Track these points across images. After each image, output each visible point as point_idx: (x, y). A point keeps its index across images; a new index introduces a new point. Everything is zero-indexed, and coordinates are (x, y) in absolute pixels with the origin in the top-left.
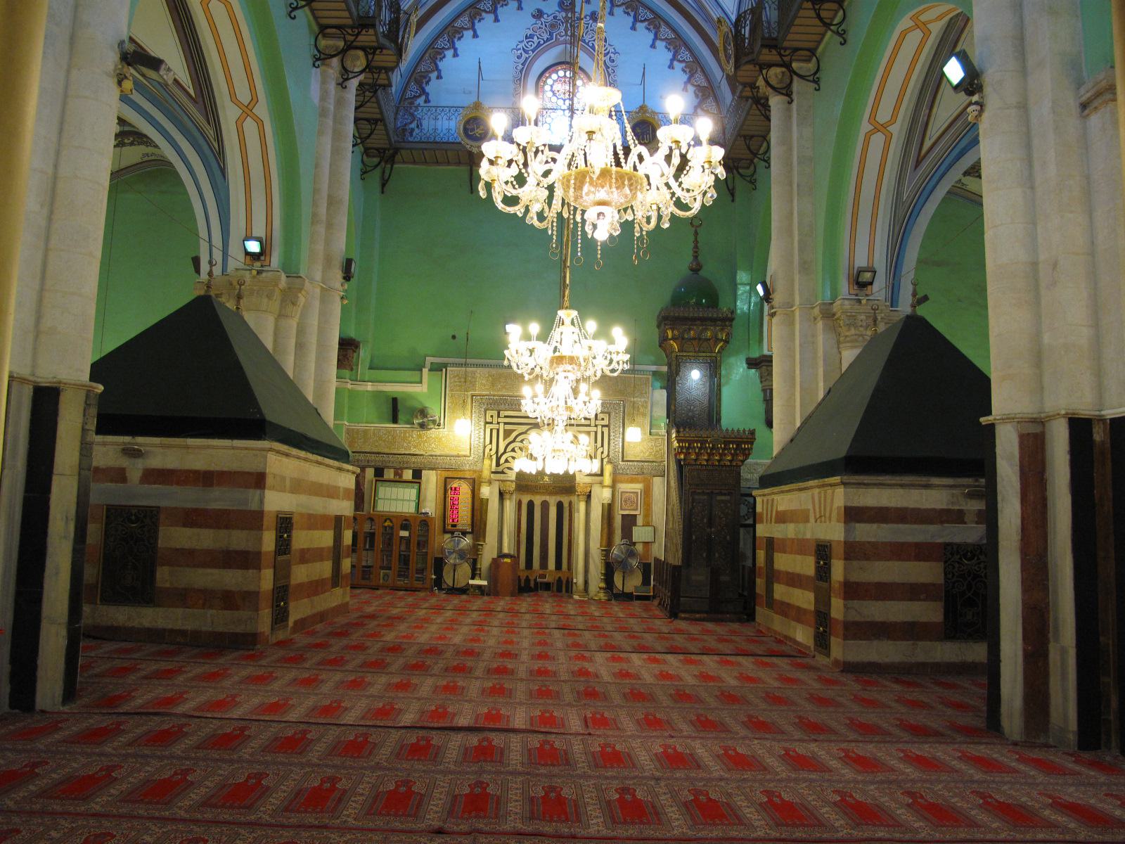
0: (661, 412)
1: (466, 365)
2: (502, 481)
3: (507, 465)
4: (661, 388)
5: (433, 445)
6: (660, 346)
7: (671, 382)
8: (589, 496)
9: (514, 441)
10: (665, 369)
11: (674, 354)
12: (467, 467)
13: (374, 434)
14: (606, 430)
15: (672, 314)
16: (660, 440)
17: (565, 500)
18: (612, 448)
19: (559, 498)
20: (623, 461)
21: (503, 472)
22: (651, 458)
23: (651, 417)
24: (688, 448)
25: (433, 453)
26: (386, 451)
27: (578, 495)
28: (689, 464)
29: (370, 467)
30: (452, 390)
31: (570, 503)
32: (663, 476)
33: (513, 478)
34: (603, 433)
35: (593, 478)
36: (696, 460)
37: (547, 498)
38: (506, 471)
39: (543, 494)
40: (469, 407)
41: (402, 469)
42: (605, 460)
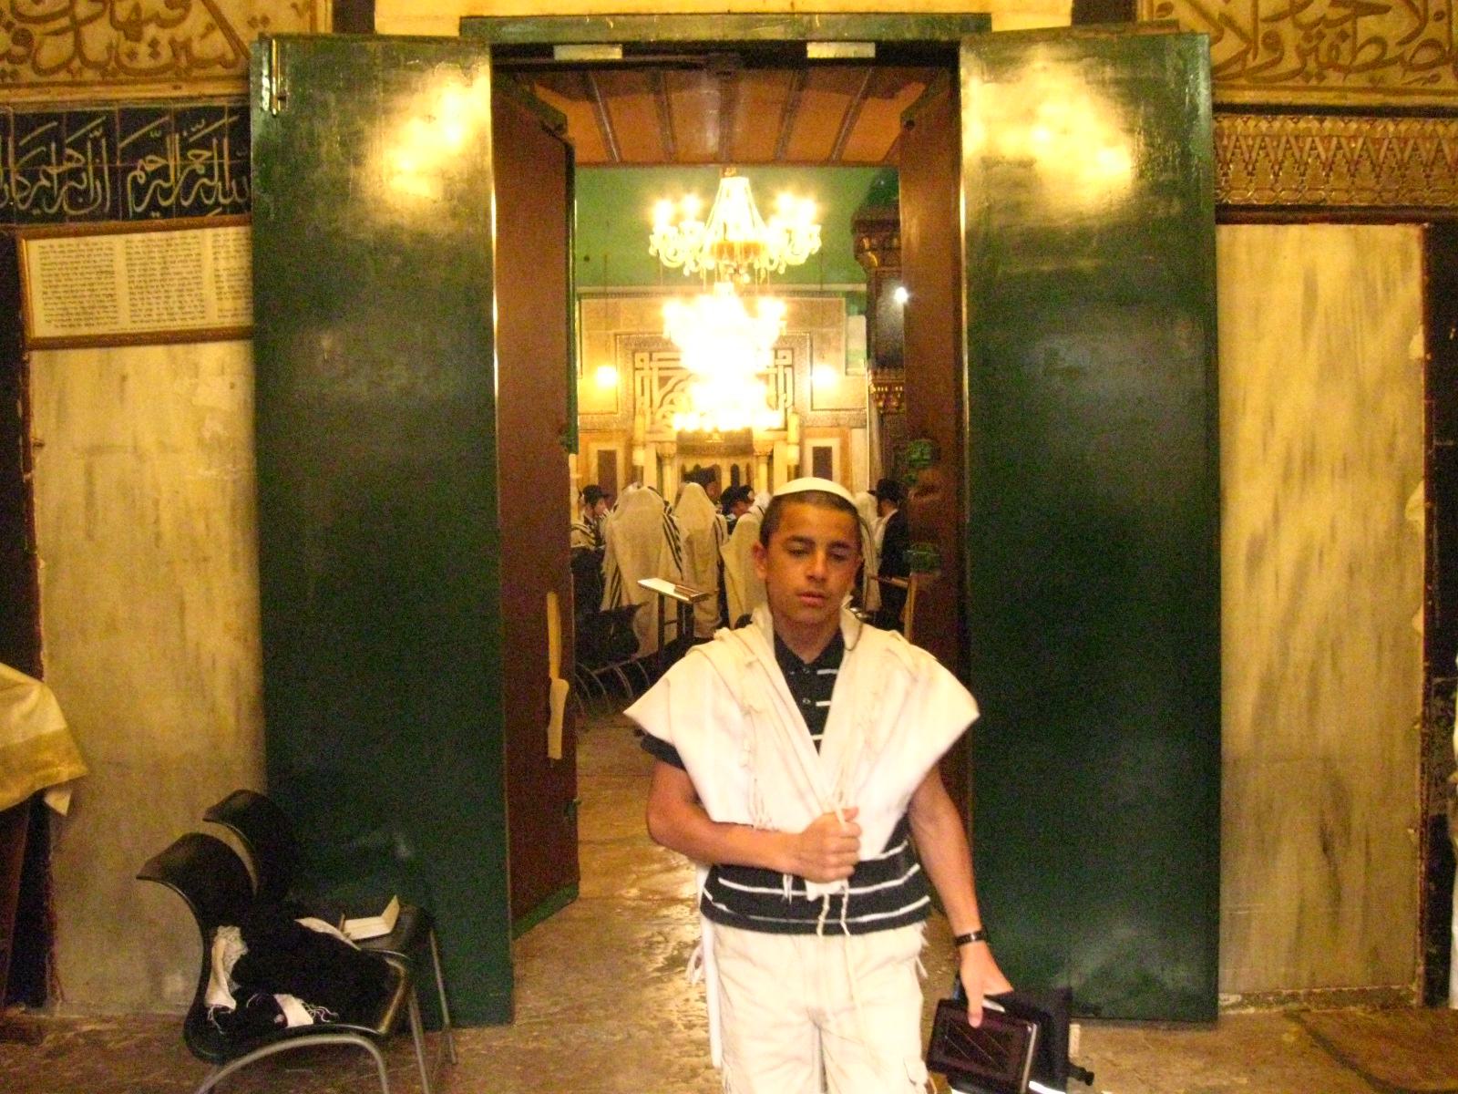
0: (859, 345)
1: (605, 295)
2: (660, 442)
4: (860, 313)
6: (856, 258)
7: (871, 306)
8: (771, 457)
9: (671, 391)
10: (863, 288)
11: (873, 270)
12: (615, 426)
15: (868, 217)
17: (742, 463)
19: (733, 461)
20: (812, 410)
23: (847, 352)
24: (887, 394)
27: (757, 457)
28: (889, 413)
30: (587, 330)
31: (748, 467)
32: (864, 427)
33: (674, 437)
34: (785, 375)
36: (898, 408)
37: (718, 461)
39: (713, 456)
40: (613, 349)
42: (790, 411)
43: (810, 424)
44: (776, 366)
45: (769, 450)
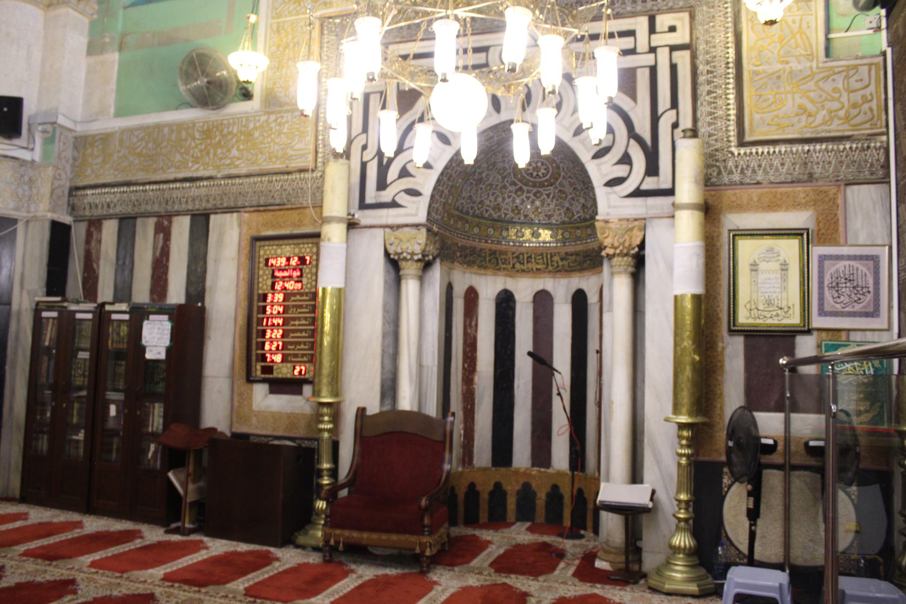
2: (391, 227)
3: (406, 183)
5: (234, 152)
8: (639, 262)
13: (121, 141)
14: (683, 59)
16: (866, 68)
18: (703, 110)
19: (577, 282)
20: (741, 144)
21: (394, 204)
22: (836, 128)
25: (234, 171)
26: (141, 176)
29: (110, 217)
34: (673, 68)
35: (651, 201)
38: (403, 199)
41: (170, 216)
43: (736, 177)
44: (653, 50)
45: (638, 241)
